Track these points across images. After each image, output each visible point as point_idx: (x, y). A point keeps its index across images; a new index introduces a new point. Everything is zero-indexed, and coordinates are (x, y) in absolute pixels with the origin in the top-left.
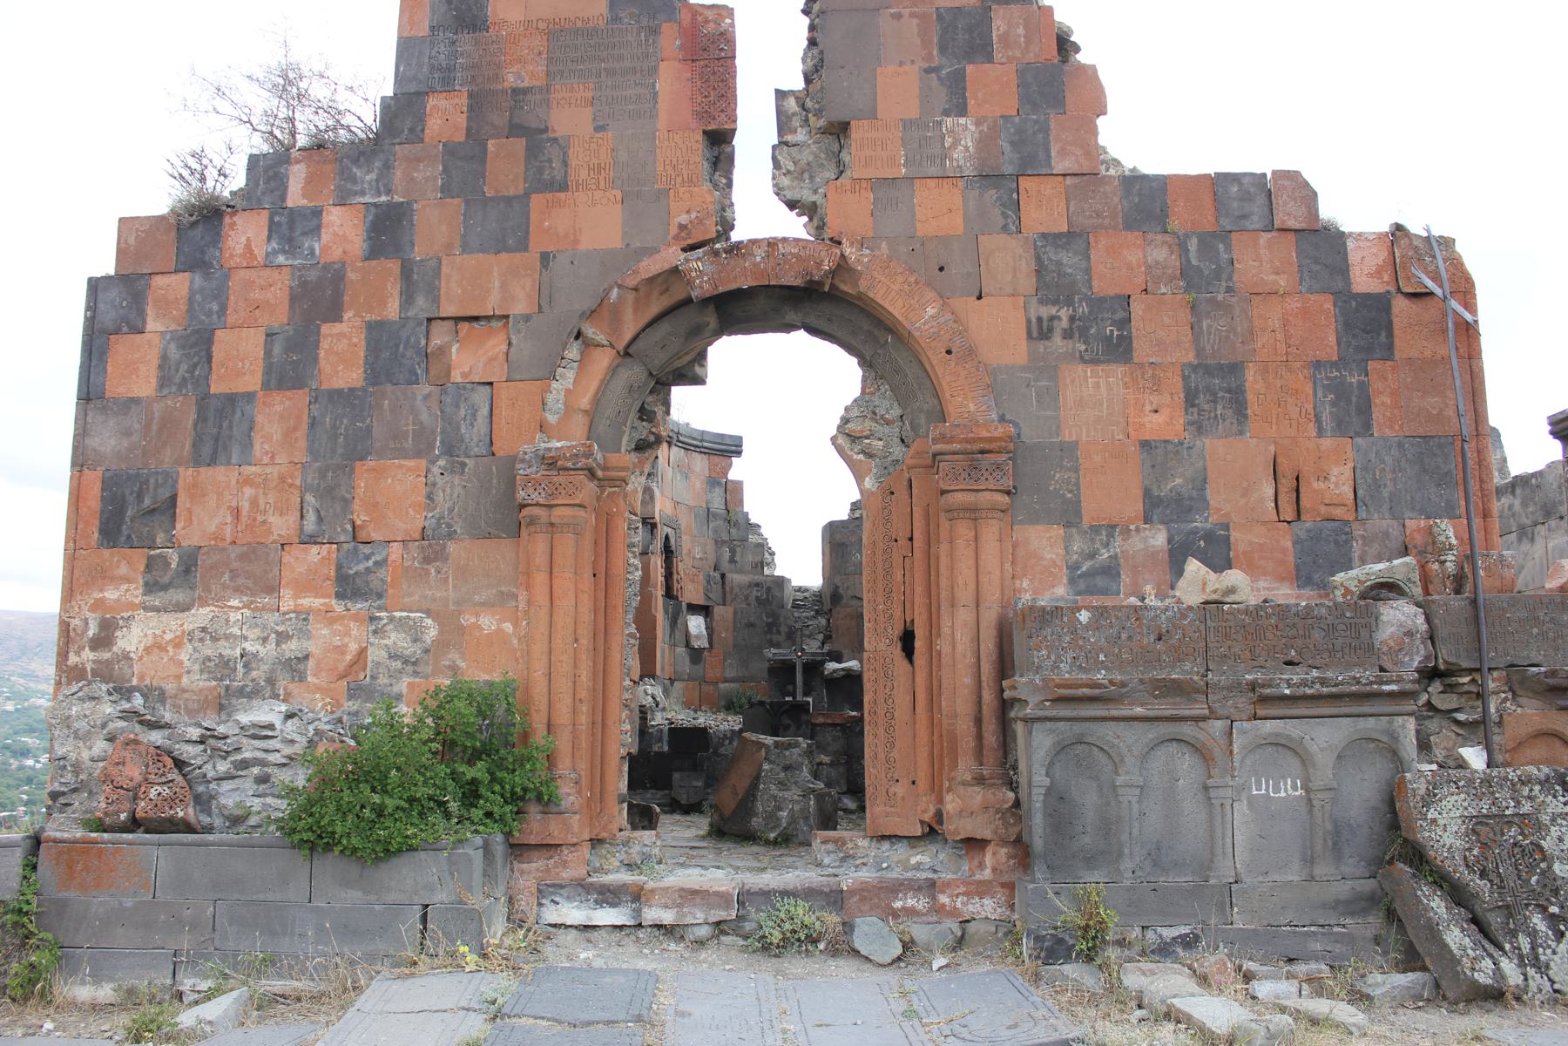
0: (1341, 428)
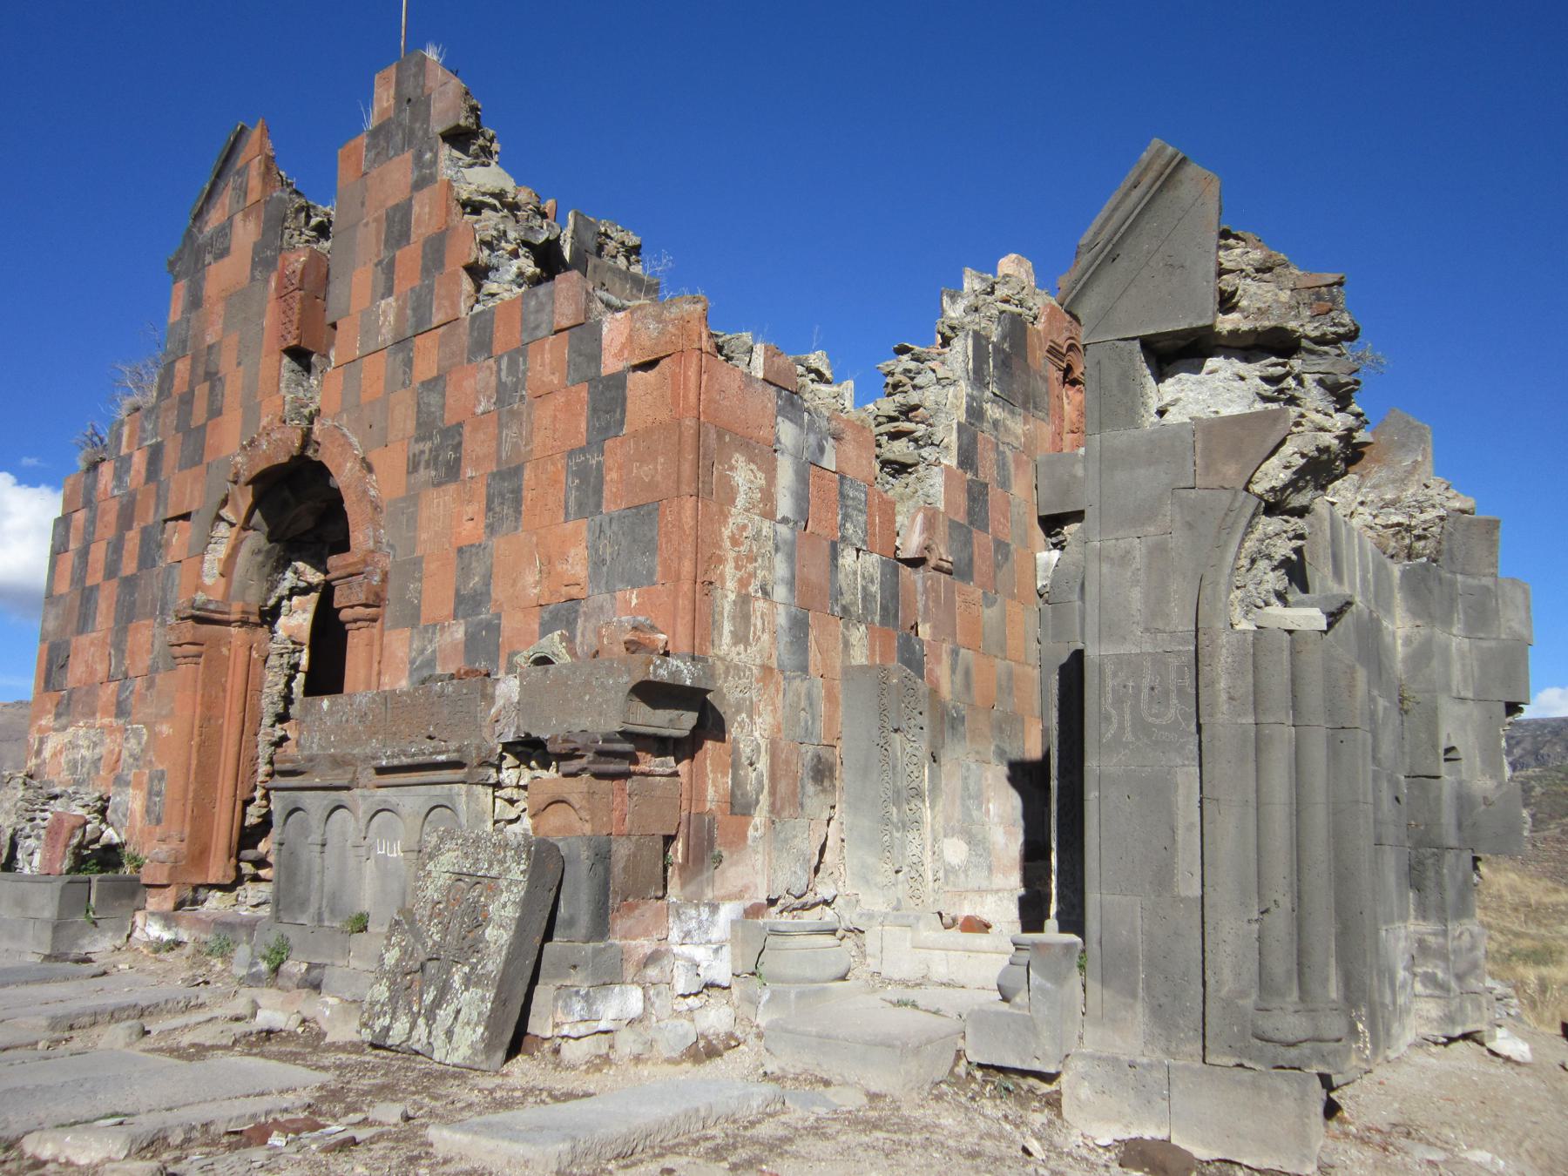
0: (582, 511)
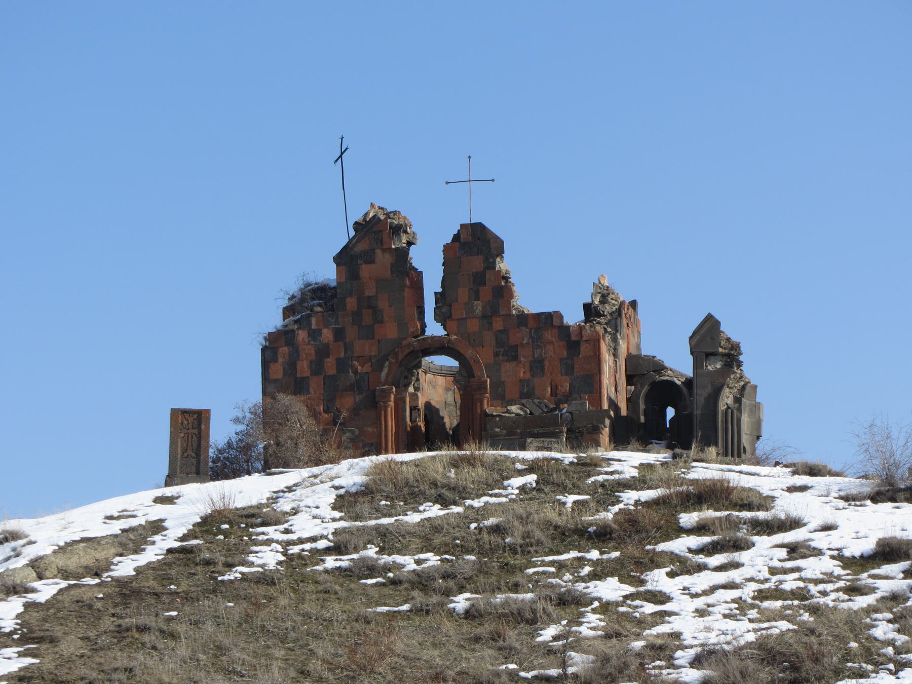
0: (566, 374)
